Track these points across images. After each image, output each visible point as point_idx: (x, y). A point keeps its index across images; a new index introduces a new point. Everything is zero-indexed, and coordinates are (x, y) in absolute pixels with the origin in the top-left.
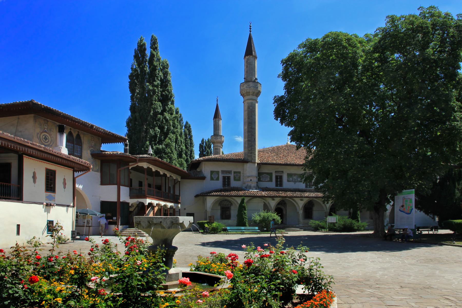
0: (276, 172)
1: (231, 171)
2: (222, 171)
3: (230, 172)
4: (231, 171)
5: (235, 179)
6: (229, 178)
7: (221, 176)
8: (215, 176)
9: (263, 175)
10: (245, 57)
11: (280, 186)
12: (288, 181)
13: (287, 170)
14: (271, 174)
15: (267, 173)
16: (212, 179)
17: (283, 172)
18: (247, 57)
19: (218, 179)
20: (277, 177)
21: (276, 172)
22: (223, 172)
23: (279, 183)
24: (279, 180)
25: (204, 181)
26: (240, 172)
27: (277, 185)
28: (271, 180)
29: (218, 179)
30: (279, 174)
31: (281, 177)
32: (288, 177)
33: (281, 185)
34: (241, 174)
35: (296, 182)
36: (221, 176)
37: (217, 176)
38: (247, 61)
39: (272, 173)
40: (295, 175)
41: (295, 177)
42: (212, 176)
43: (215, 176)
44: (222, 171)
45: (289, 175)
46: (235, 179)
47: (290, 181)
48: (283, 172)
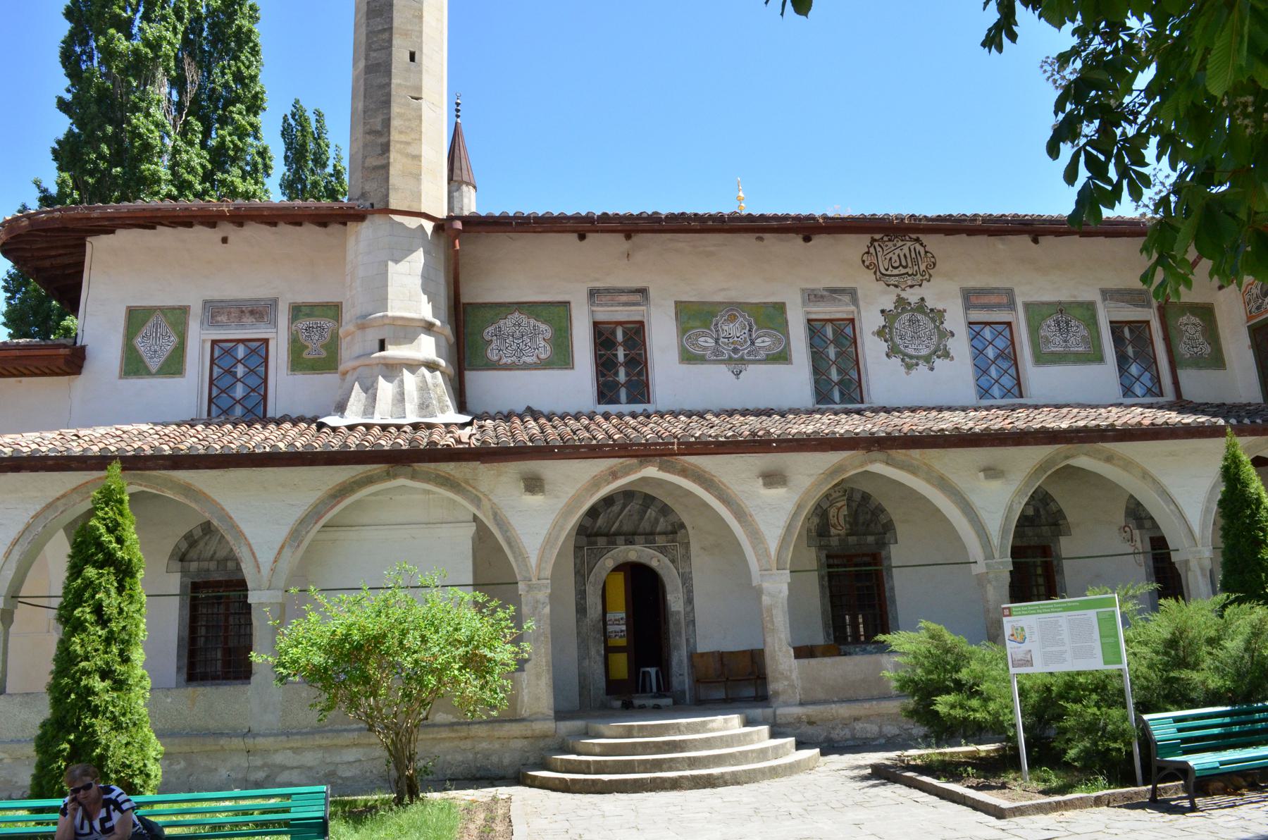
0: (593, 294)
1: (275, 302)
2: (206, 302)
3: (260, 311)
4: (275, 302)
5: (299, 363)
7: (198, 339)
8: (154, 348)
9: (507, 324)
11: (631, 400)
12: (688, 357)
13: (666, 286)
14: (557, 314)
16: (133, 365)
19: (174, 365)
21: (593, 294)
22: (215, 311)
23: (622, 377)
24: (621, 363)
25: (78, 382)
26: (334, 310)
27: (606, 393)
28: (562, 357)
29: (174, 365)
31: (636, 333)
32: (683, 330)
33: (640, 390)
36: (198, 339)
40: (733, 309)
41: (734, 330)
42: (138, 342)
45: (694, 316)
46: (299, 363)
47: (701, 359)
48: (643, 291)
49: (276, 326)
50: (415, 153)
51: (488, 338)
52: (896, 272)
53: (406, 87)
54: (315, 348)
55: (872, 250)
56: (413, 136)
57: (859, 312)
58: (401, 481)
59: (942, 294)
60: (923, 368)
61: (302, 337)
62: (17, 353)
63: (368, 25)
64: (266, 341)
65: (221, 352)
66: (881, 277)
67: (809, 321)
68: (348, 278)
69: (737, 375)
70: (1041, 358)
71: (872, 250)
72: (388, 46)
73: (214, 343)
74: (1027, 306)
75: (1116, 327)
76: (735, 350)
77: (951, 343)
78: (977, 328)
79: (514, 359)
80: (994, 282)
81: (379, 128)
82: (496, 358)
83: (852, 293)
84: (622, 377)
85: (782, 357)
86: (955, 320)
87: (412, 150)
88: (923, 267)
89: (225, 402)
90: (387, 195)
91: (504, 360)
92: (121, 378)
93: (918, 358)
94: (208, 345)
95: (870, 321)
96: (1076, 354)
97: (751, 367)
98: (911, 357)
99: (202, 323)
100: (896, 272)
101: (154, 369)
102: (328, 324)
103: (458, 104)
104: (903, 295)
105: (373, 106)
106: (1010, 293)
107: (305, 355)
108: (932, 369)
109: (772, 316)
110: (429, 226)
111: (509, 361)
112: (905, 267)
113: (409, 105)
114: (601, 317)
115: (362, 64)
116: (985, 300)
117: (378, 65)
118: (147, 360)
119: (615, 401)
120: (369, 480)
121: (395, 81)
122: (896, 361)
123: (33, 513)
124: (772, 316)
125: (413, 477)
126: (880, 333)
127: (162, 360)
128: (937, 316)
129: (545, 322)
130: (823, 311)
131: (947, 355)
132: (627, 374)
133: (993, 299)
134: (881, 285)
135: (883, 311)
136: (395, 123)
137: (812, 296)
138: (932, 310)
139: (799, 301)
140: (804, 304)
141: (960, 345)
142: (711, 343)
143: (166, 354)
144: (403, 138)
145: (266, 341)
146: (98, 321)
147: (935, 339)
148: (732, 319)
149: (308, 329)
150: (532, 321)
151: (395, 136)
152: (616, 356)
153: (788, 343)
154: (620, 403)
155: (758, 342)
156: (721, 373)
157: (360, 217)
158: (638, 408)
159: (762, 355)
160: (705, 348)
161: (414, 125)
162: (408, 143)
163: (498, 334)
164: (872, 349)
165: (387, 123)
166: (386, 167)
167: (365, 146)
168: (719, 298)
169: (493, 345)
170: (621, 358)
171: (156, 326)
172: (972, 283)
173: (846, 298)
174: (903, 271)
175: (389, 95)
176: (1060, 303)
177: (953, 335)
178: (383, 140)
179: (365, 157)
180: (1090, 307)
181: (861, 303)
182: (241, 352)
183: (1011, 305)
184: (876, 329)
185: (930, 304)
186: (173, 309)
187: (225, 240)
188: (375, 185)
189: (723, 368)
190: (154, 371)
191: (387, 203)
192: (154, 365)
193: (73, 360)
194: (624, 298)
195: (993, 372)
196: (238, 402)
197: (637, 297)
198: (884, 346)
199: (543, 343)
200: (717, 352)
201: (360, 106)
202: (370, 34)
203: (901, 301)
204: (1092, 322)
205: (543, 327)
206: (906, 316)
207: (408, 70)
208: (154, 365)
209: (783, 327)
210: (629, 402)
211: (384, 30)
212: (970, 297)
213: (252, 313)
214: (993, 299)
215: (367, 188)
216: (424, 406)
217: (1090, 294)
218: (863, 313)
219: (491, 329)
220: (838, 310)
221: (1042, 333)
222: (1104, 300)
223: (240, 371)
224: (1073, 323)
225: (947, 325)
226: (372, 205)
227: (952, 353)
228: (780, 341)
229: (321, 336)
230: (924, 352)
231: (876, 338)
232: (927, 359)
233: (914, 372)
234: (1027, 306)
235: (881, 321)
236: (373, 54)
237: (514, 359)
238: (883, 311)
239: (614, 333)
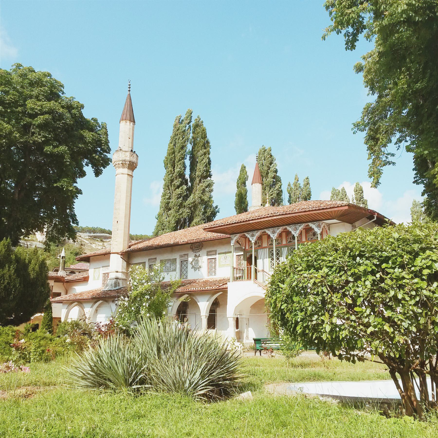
17: (156, 258)
21: (149, 259)
41: (168, 265)
66: (193, 250)
83: (187, 255)
85: (175, 270)
106: (216, 251)
114: (150, 264)
116: (211, 253)
133: (213, 253)
137: (181, 256)
164: (190, 266)
173: (186, 256)
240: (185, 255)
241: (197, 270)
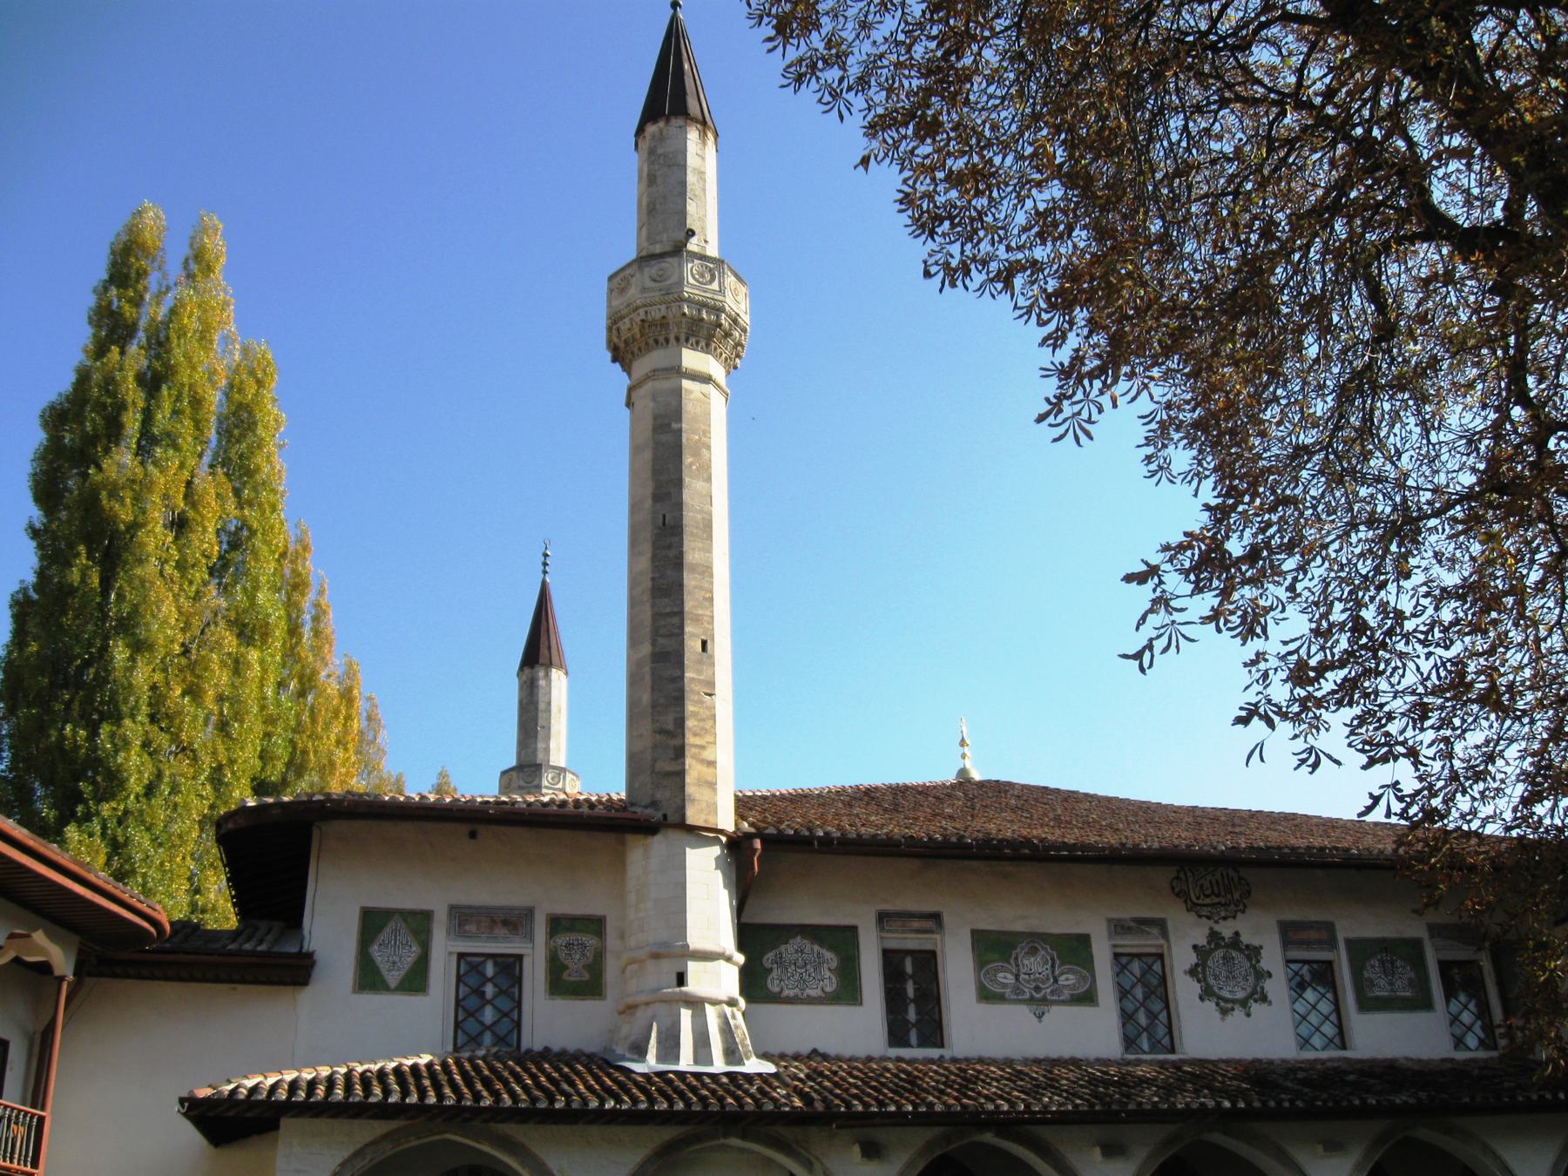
2: (454, 910)
3: (515, 921)
5: (559, 985)
6: (510, 967)
8: (394, 958)
9: (789, 949)
10: (640, 131)
11: (923, 1043)
14: (842, 940)
15: (815, 933)
16: (369, 978)
17: (936, 917)
18: (651, 129)
19: (416, 981)
20: (891, 961)
21: (883, 918)
22: (462, 917)
23: (912, 1015)
25: (307, 998)
26: (596, 925)
27: (897, 1035)
28: (848, 991)
29: (416, 981)
30: (912, 942)
31: (928, 962)
32: (980, 964)
33: (933, 1032)
34: (612, 941)
35: (1044, 1001)
37: (410, 955)
38: (652, 152)
39: (853, 929)
40: (1036, 940)
41: (1035, 965)
42: (375, 951)
43: (394, 958)
44: (454, 910)
45: (992, 947)
46: (559, 985)
47: (1000, 998)
48: (936, 917)
49: (532, 940)
50: (711, 758)
51: (768, 965)
52: (1208, 901)
53: (700, 681)
54: (575, 970)
55: (1182, 875)
56: (709, 738)
57: (1169, 948)
58: (735, 1142)
59: (1258, 928)
60: (1239, 1013)
61: (562, 955)
62: (254, 960)
63: (653, 606)
64: (520, 958)
65: (468, 966)
66: (1192, 907)
67: (1117, 956)
68: (632, 898)
69: (1040, 1017)
70: (1367, 1004)
71: (1182, 875)
72: (678, 634)
73: (461, 956)
74: (1348, 942)
75: (1444, 966)
76: (1037, 989)
77: (1269, 986)
78: (1294, 967)
79: (797, 991)
80: (1313, 915)
81: (671, 727)
82: (776, 989)
83: (1161, 924)
84: (912, 1015)
85: (1087, 998)
86: (1272, 958)
87: (707, 755)
88: (1237, 896)
89: (472, 1026)
90: (683, 807)
91: (786, 992)
92: (354, 991)
93: (1233, 1001)
94: (454, 958)
95: (1182, 957)
96: (1404, 999)
97: (1054, 1009)
98: (1226, 1000)
99: (448, 932)
100: (1208, 901)
101: (393, 983)
102: (591, 941)
103: (546, 555)
104: (1217, 928)
105: (662, 701)
106: (1330, 927)
107: (565, 976)
108: (1248, 1015)
109: (1075, 949)
110: (724, 839)
111: (791, 993)
112: (1218, 896)
113: (701, 702)
115: (646, 649)
117: (668, 653)
118: (385, 973)
119: (906, 1044)
120: (698, 1138)
121: (688, 675)
122: (1210, 1005)
123: (339, 1161)
124: (1075, 949)
125: (744, 1136)
126: (1192, 972)
127: (403, 973)
128: (1254, 953)
129: (831, 948)
130: (1132, 943)
131: (1264, 998)
132: (918, 1013)
133: (1313, 935)
134: (1192, 917)
135: (1195, 947)
136: (690, 723)
137: (1119, 928)
138: (1247, 946)
139: (1105, 933)
140: (1110, 937)
141: (1277, 987)
142: (1010, 979)
143: (407, 967)
144: (697, 741)
145: (520, 958)
146: (329, 924)
147: (1251, 979)
148: (1033, 951)
149: (569, 945)
150: (816, 948)
151: (690, 739)
152: (905, 989)
153: (1094, 981)
154: (910, 1046)
155: (1062, 980)
156: (1023, 1013)
157: (649, 828)
158: (934, 1053)
159: (1066, 994)
160: (1005, 986)
161: (708, 725)
162: (703, 747)
163: (779, 961)
164: (1185, 990)
165: (680, 722)
166: (681, 774)
167: (655, 747)
168: (1019, 927)
169: (774, 974)
170: (910, 992)
171: (395, 931)
172: (1292, 915)
173: (1155, 931)
174: (1216, 900)
175: (682, 691)
176: (1383, 940)
177: (1270, 975)
178: (677, 742)
179: (655, 760)
180: (1416, 944)
181: (1172, 937)
182: (490, 970)
183: (1331, 943)
184: (1188, 967)
185: (1246, 939)
186: (413, 913)
187: (473, 835)
188: (668, 794)
189: (1023, 1010)
190: (393, 984)
191: (683, 816)
192: (393, 978)
193: (295, 971)
194: (916, 924)
195: (1314, 1018)
196: (488, 1028)
197: (930, 924)
198: (1196, 988)
199: (828, 974)
200: (1017, 990)
201: (646, 698)
202: (656, 616)
203: (1214, 936)
204: (1419, 963)
205: (828, 955)
206: (1219, 953)
207: (700, 662)
208: (393, 978)
209: (1087, 962)
210: (919, 1046)
211: (675, 614)
212: (1290, 933)
213: (505, 923)
214: (1313, 935)
215: (659, 796)
216: (731, 1053)
217: (1414, 929)
218: (1175, 950)
219: (770, 955)
220: (1145, 943)
221: (1366, 975)
222: (1432, 937)
223: (489, 990)
224: (1398, 963)
225: (1264, 964)
226: (665, 816)
227: (1270, 996)
228: (1084, 978)
229: (583, 955)
230: (1240, 995)
231: (1188, 978)
232: (1244, 1003)
233: (1229, 1018)
234: (1348, 942)
235: (1192, 958)
236: (661, 641)
237: (797, 991)
238: (1195, 947)
239: (903, 960)
240: (1142, 922)
241: (1239, 1013)
